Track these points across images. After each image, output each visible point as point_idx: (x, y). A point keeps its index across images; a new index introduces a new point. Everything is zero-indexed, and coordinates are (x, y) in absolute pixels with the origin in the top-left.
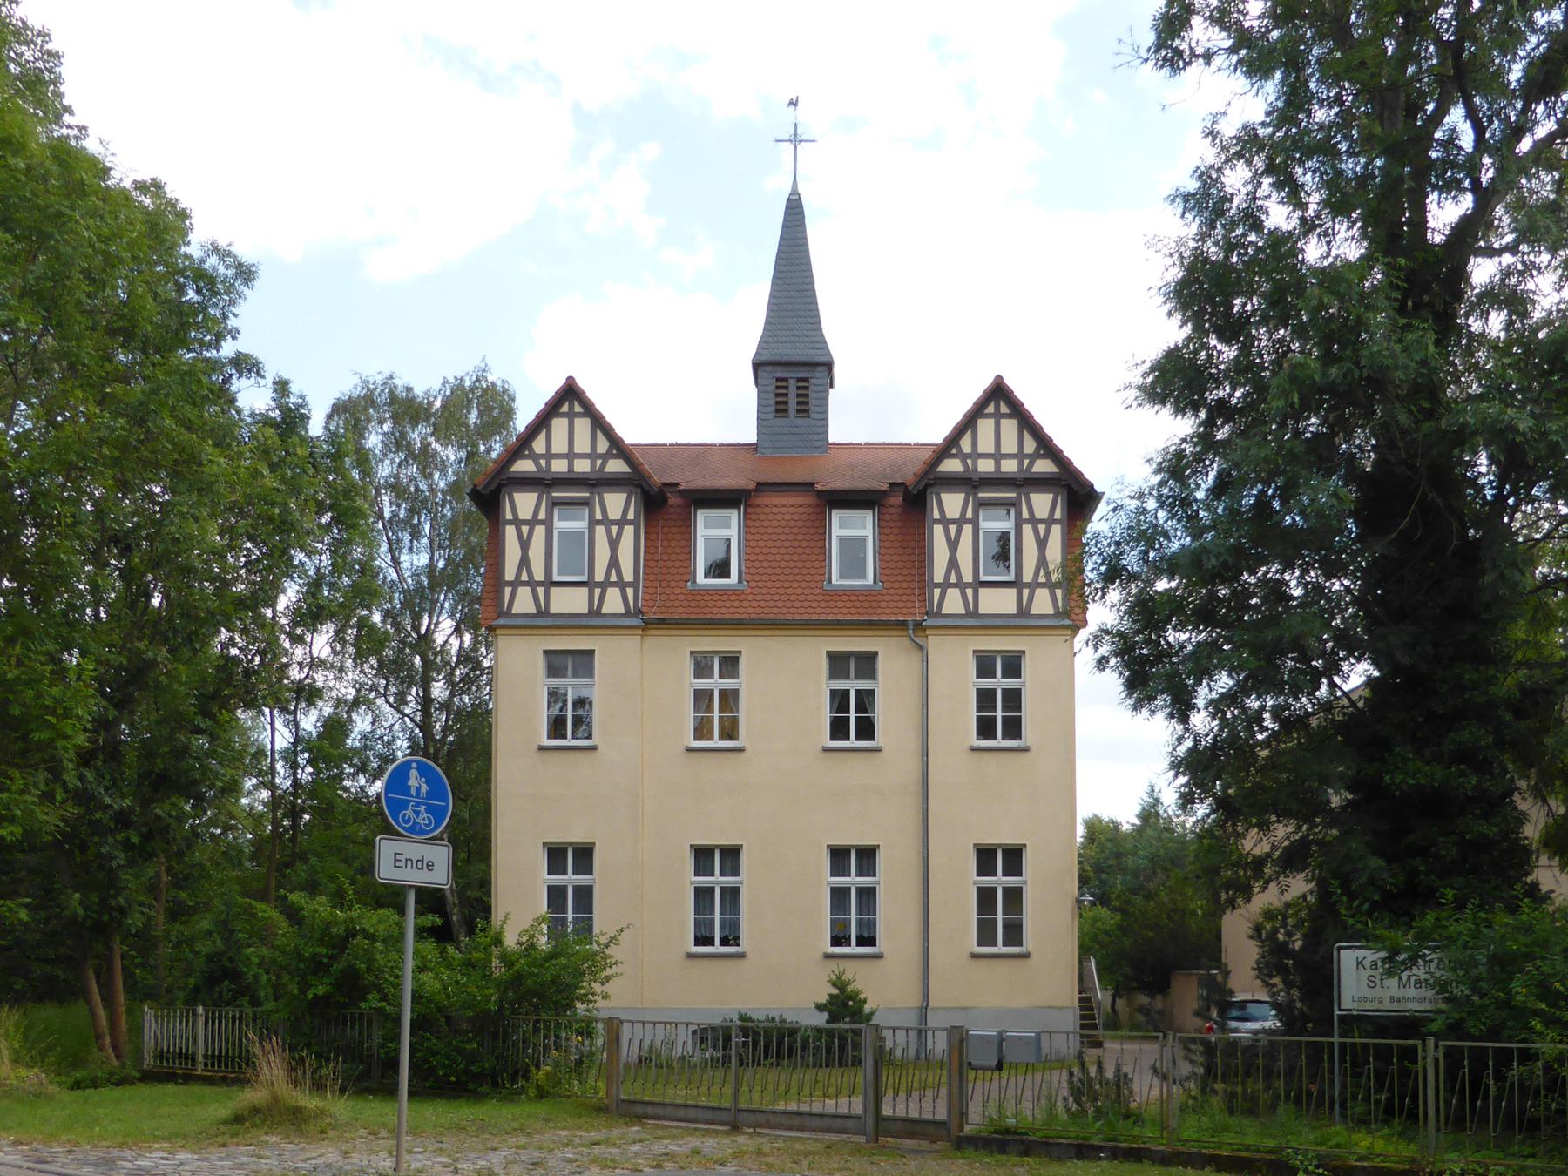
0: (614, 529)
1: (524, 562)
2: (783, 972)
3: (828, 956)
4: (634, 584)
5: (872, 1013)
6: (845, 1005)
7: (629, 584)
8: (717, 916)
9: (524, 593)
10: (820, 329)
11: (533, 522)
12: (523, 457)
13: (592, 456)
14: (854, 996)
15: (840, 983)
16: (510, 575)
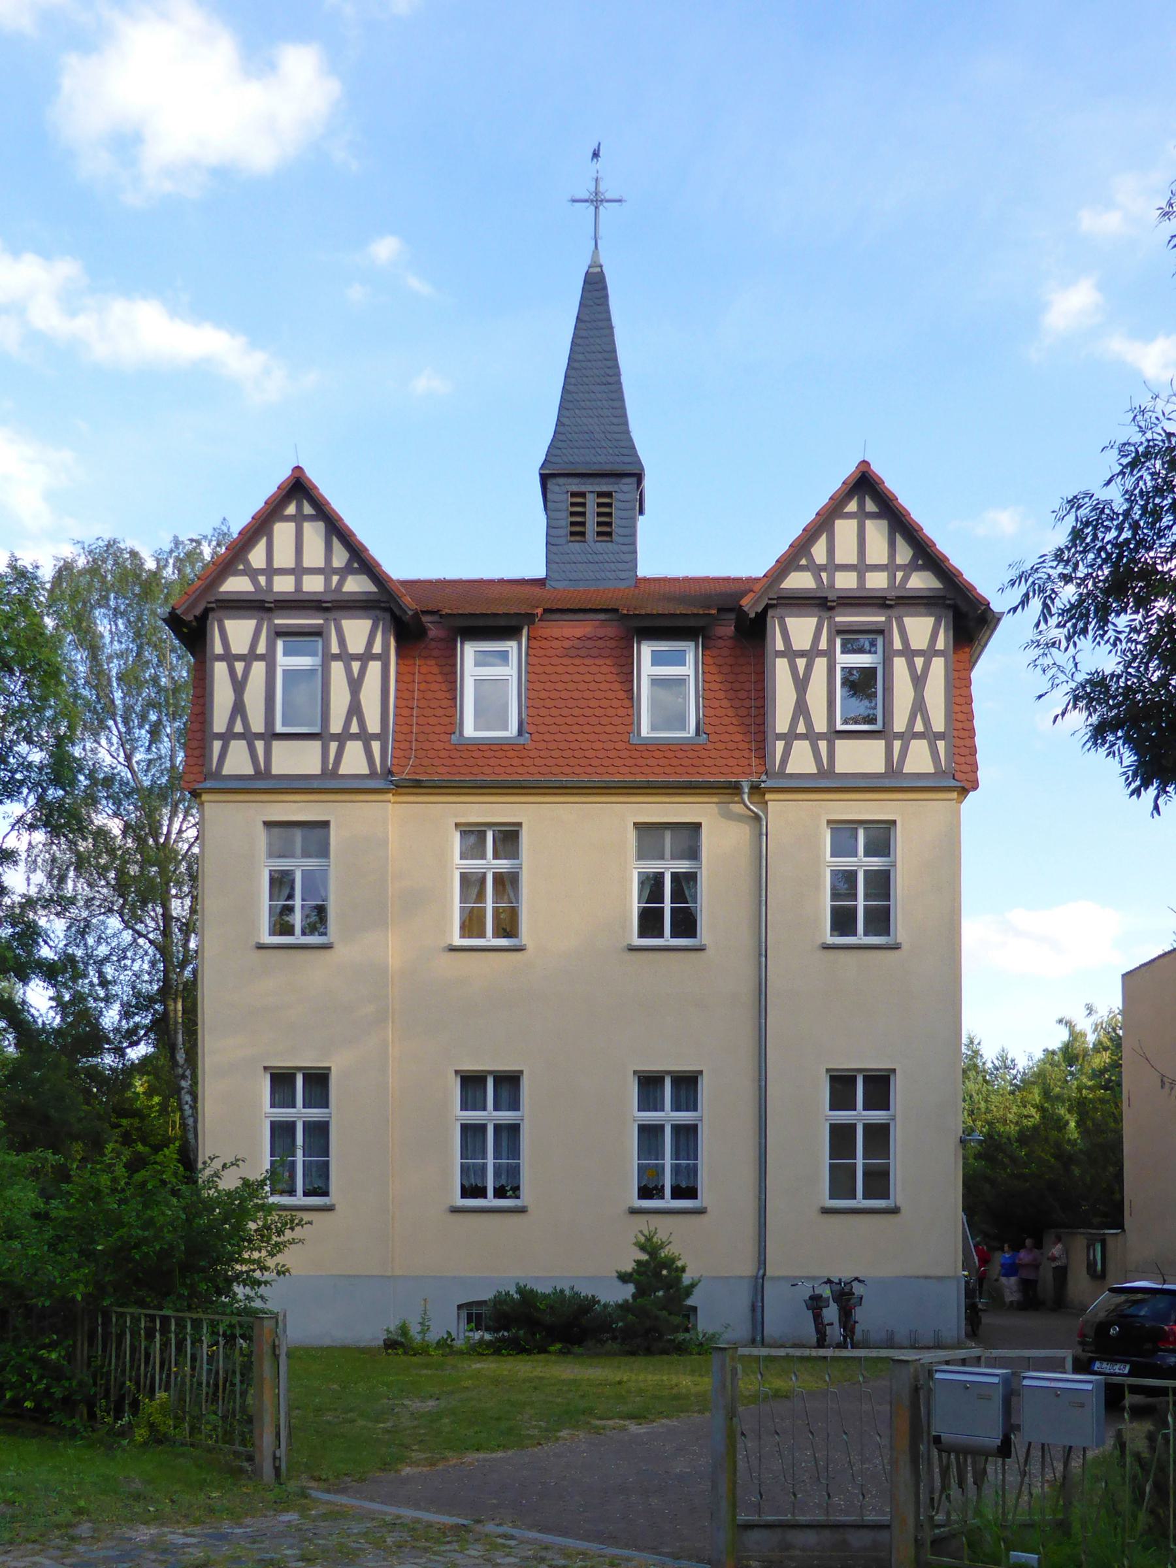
0: (356, 666)
1: (239, 708)
2: (576, 1230)
3: (634, 1211)
4: (381, 737)
5: (693, 1285)
6: (658, 1274)
7: (375, 737)
8: (490, 1161)
9: (238, 748)
10: (628, 432)
11: (251, 657)
12: (237, 573)
13: (326, 571)
14: (669, 1263)
15: (649, 1246)
16: (219, 726)
